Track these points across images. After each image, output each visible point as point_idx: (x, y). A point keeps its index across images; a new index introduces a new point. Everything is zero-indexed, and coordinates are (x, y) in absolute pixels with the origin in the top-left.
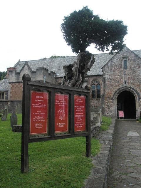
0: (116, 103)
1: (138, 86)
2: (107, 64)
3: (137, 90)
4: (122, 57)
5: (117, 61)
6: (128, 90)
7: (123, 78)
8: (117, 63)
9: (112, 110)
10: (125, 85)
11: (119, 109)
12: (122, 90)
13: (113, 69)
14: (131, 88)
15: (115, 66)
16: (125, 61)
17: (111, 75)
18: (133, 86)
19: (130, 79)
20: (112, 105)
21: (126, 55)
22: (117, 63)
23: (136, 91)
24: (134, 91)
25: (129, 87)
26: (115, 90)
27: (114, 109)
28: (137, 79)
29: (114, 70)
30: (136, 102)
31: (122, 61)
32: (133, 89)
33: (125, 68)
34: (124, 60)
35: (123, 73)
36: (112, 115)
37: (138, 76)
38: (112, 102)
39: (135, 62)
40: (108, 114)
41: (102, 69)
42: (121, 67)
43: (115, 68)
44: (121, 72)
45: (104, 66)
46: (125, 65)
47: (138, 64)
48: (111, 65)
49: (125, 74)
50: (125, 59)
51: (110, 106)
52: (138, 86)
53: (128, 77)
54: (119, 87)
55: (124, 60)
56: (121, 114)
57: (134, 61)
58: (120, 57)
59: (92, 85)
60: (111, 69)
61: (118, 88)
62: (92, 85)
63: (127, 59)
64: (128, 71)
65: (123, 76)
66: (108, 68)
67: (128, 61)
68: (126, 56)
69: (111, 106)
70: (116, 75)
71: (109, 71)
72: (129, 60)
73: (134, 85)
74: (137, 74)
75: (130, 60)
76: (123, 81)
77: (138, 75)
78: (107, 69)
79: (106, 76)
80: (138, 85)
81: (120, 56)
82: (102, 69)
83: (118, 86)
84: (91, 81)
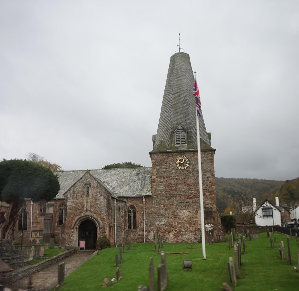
0: (77, 233)
1: (99, 215)
2: (70, 190)
4: (85, 184)
5: (79, 188)
7: (85, 207)
8: (79, 190)
9: (72, 240)
10: (86, 214)
11: (80, 238)
12: (84, 218)
13: (75, 196)
14: (92, 217)
15: (77, 193)
16: (88, 188)
18: (94, 215)
19: (92, 208)
20: (72, 235)
21: (88, 182)
22: (79, 190)
23: (97, 221)
24: (95, 220)
25: (90, 216)
26: (76, 219)
27: (75, 239)
28: (99, 207)
29: (76, 197)
30: (97, 232)
31: (84, 188)
32: (94, 218)
34: (86, 186)
35: (85, 201)
36: (72, 246)
37: (100, 205)
38: (73, 232)
39: (97, 190)
40: (68, 245)
41: (64, 195)
42: (83, 194)
43: (77, 195)
44: (83, 200)
45: (66, 193)
46: (88, 192)
47: (99, 192)
48: (74, 191)
50: (88, 186)
51: (70, 236)
52: (99, 215)
53: (89, 205)
54: (81, 216)
55: (86, 186)
56: (82, 244)
57: (97, 188)
58: (82, 183)
59: (59, 209)
60: (74, 196)
61: (79, 216)
62: (59, 209)
63: (89, 186)
66: (70, 194)
67: (90, 188)
68: (89, 183)
69: (71, 236)
70: (77, 203)
71: (71, 198)
72: (92, 187)
73: (95, 213)
74: (98, 202)
75: (93, 187)
76: (85, 209)
77: (99, 203)
78: (69, 196)
80: (99, 215)
81: (82, 182)
83: (80, 215)
84: (58, 205)
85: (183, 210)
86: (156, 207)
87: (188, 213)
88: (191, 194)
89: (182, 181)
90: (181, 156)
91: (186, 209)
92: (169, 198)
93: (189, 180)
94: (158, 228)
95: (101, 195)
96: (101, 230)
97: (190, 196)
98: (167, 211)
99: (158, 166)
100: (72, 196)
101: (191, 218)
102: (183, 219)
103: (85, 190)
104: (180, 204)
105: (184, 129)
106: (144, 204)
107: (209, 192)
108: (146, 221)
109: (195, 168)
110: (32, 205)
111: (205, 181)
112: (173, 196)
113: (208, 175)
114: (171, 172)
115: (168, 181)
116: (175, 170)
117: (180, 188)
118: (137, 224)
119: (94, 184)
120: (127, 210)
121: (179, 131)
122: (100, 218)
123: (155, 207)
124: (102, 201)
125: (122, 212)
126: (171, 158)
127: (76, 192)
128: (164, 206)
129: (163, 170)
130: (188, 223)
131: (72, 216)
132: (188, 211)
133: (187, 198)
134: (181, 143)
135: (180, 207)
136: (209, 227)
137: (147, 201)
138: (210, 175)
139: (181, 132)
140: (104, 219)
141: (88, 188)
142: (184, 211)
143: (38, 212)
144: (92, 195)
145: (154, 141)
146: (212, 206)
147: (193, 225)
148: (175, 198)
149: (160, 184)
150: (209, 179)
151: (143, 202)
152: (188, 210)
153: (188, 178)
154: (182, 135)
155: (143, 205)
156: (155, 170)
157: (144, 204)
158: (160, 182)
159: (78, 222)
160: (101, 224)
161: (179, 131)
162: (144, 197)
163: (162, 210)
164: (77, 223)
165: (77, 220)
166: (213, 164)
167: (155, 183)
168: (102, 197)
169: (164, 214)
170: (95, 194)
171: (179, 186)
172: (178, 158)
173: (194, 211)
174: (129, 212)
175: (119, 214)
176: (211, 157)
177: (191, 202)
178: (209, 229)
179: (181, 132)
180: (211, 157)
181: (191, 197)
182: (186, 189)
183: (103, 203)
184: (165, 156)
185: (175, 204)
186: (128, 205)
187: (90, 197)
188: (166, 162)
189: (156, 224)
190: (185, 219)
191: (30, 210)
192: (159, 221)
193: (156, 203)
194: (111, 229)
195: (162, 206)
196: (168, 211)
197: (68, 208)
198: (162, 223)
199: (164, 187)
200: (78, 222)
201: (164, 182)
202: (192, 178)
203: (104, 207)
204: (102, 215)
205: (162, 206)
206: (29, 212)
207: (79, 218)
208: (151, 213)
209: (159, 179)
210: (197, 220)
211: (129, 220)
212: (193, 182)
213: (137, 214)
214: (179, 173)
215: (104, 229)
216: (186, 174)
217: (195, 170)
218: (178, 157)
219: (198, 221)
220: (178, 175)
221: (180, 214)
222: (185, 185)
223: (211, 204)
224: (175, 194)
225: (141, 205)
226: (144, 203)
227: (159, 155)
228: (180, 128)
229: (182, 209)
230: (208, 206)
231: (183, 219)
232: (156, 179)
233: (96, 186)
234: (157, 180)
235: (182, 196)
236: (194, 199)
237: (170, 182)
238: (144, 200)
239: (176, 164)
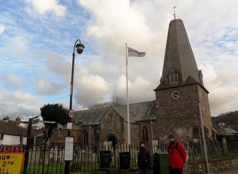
2: (102, 118)
3: (117, 136)
6: (110, 136)
10: (111, 132)
13: (105, 122)
14: (114, 134)
17: (104, 125)
18: (115, 133)
23: (117, 137)
24: (115, 137)
25: (113, 134)
26: (105, 136)
29: (105, 123)
33: (112, 121)
35: (110, 125)
43: (106, 121)
46: (111, 119)
47: (118, 119)
48: (104, 120)
49: (111, 125)
52: (118, 133)
55: (111, 116)
57: (116, 116)
60: (104, 122)
61: (107, 134)
64: (112, 123)
65: (110, 126)
66: (102, 121)
73: (115, 132)
74: (117, 125)
78: (102, 122)
79: (101, 127)
82: (99, 122)
85: (179, 128)
86: (160, 127)
87: (182, 131)
88: (183, 117)
89: (177, 107)
90: (174, 90)
91: (180, 128)
93: (181, 107)
94: (162, 142)
95: (118, 121)
96: (119, 142)
97: (182, 118)
98: (167, 129)
99: (160, 99)
100: (103, 122)
101: (184, 134)
102: (178, 135)
103: (110, 118)
104: (176, 124)
105: (175, 72)
107: (196, 114)
108: (154, 137)
109: (184, 98)
110: (90, 129)
111: (192, 106)
112: (171, 119)
113: (195, 102)
114: (168, 102)
115: (167, 108)
116: (171, 101)
117: (176, 113)
118: (148, 139)
119: (114, 114)
120: (141, 130)
121: (172, 73)
122: (118, 135)
123: (159, 127)
124: (119, 124)
125: (137, 132)
127: (105, 120)
128: (165, 126)
130: (182, 138)
131: (103, 134)
132: (182, 129)
133: (181, 120)
135: (176, 126)
136: (196, 140)
137: (154, 123)
138: (196, 102)
139: (173, 74)
140: (120, 135)
141: (111, 116)
142: (179, 129)
143: (93, 133)
144: (114, 121)
145: (160, 82)
146: (199, 125)
147: (186, 139)
148: (172, 120)
149: (162, 111)
150: (196, 104)
151: (151, 124)
152: (182, 129)
153: (181, 105)
154: (174, 76)
156: (158, 102)
159: (107, 138)
160: (119, 139)
161: (172, 73)
163: (164, 129)
164: (106, 139)
165: (106, 137)
166: (198, 93)
167: (159, 111)
168: (119, 122)
169: (165, 132)
170: (115, 120)
171: (175, 111)
172: (172, 92)
173: (186, 129)
174: (143, 131)
175: (135, 133)
176: (196, 89)
177: (184, 122)
178: (196, 142)
179: (173, 74)
180: (196, 89)
181: (183, 119)
183: (119, 126)
185: (172, 124)
186: (142, 126)
187: (113, 122)
188: (165, 95)
189: (161, 139)
190: (180, 135)
191: (89, 132)
192: (163, 137)
193: (160, 124)
194: (124, 142)
195: (164, 126)
196: (168, 129)
197: (101, 129)
198: (165, 138)
200: (107, 138)
201: (164, 109)
202: (183, 105)
203: (120, 128)
204: (119, 133)
205: (164, 126)
206: (89, 133)
207: (107, 135)
208: (157, 132)
209: (161, 108)
210: (189, 135)
211: (144, 137)
212: (184, 108)
213: (148, 133)
214: (174, 103)
215: (120, 142)
216: (178, 102)
217: (185, 99)
219: (189, 136)
221: (176, 132)
223: (198, 123)
224: (172, 117)
225: (150, 126)
226: (152, 124)
228: (172, 71)
229: (178, 128)
230: (196, 125)
231: (178, 135)
233: (115, 115)
234: (160, 108)
235: (177, 118)
236: (186, 120)
237: (168, 109)
238: (152, 123)
239: (172, 96)
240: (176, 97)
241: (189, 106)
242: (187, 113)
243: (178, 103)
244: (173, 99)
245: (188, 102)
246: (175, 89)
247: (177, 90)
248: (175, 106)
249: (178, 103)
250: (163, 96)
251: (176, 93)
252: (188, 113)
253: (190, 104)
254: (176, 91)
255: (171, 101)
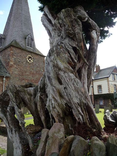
88: (34, 80)
89: (29, 70)
90: (29, 55)
92: (21, 80)
93: (33, 71)
97: (33, 81)
99: (15, 56)
105: (32, 39)
106: (4, 82)
112: (23, 79)
114: (23, 62)
115: (21, 68)
116: (25, 63)
117: (27, 75)
126: (24, 53)
129: (18, 60)
134: (29, 46)
138: (43, 71)
148: (24, 81)
151: (3, 81)
153: (32, 69)
155: (3, 83)
156: (13, 59)
157: (4, 82)
158: (16, 68)
162: (6, 76)
171: (27, 73)
182: (31, 76)
184: (20, 51)
193: (12, 82)
199: (18, 72)
202: (34, 70)
209: (15, 66)
212: (35, 72)
218: (27, 54)
220: (27, 66)
222: (30, 73)
224: (25, 78)
226: (4, 81)
227: (16, 49)
232: (13, 65)
235: (28, 80)
237: (22, 69)
238: (4, 79)
240: (30, 61)
241: (38, 72)
242: (36, 77)
243: (30, 67)
244: (27, 61)
245: (38, 68)
246: (30, 53)
247: (31, 55)
248: (28, 68)
249: (30, 67)
250: (19, 55)
251: (30, 57)
252: (37, 78)
253: (39, 71)
254: (30, 56)
255: (25, 63)
